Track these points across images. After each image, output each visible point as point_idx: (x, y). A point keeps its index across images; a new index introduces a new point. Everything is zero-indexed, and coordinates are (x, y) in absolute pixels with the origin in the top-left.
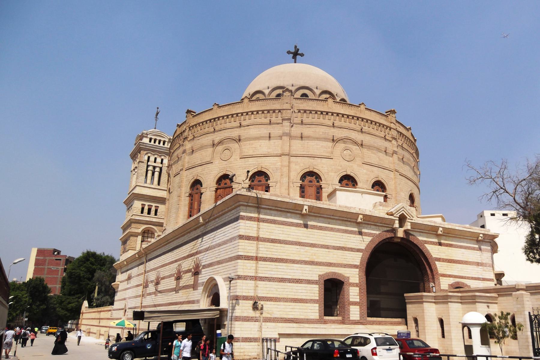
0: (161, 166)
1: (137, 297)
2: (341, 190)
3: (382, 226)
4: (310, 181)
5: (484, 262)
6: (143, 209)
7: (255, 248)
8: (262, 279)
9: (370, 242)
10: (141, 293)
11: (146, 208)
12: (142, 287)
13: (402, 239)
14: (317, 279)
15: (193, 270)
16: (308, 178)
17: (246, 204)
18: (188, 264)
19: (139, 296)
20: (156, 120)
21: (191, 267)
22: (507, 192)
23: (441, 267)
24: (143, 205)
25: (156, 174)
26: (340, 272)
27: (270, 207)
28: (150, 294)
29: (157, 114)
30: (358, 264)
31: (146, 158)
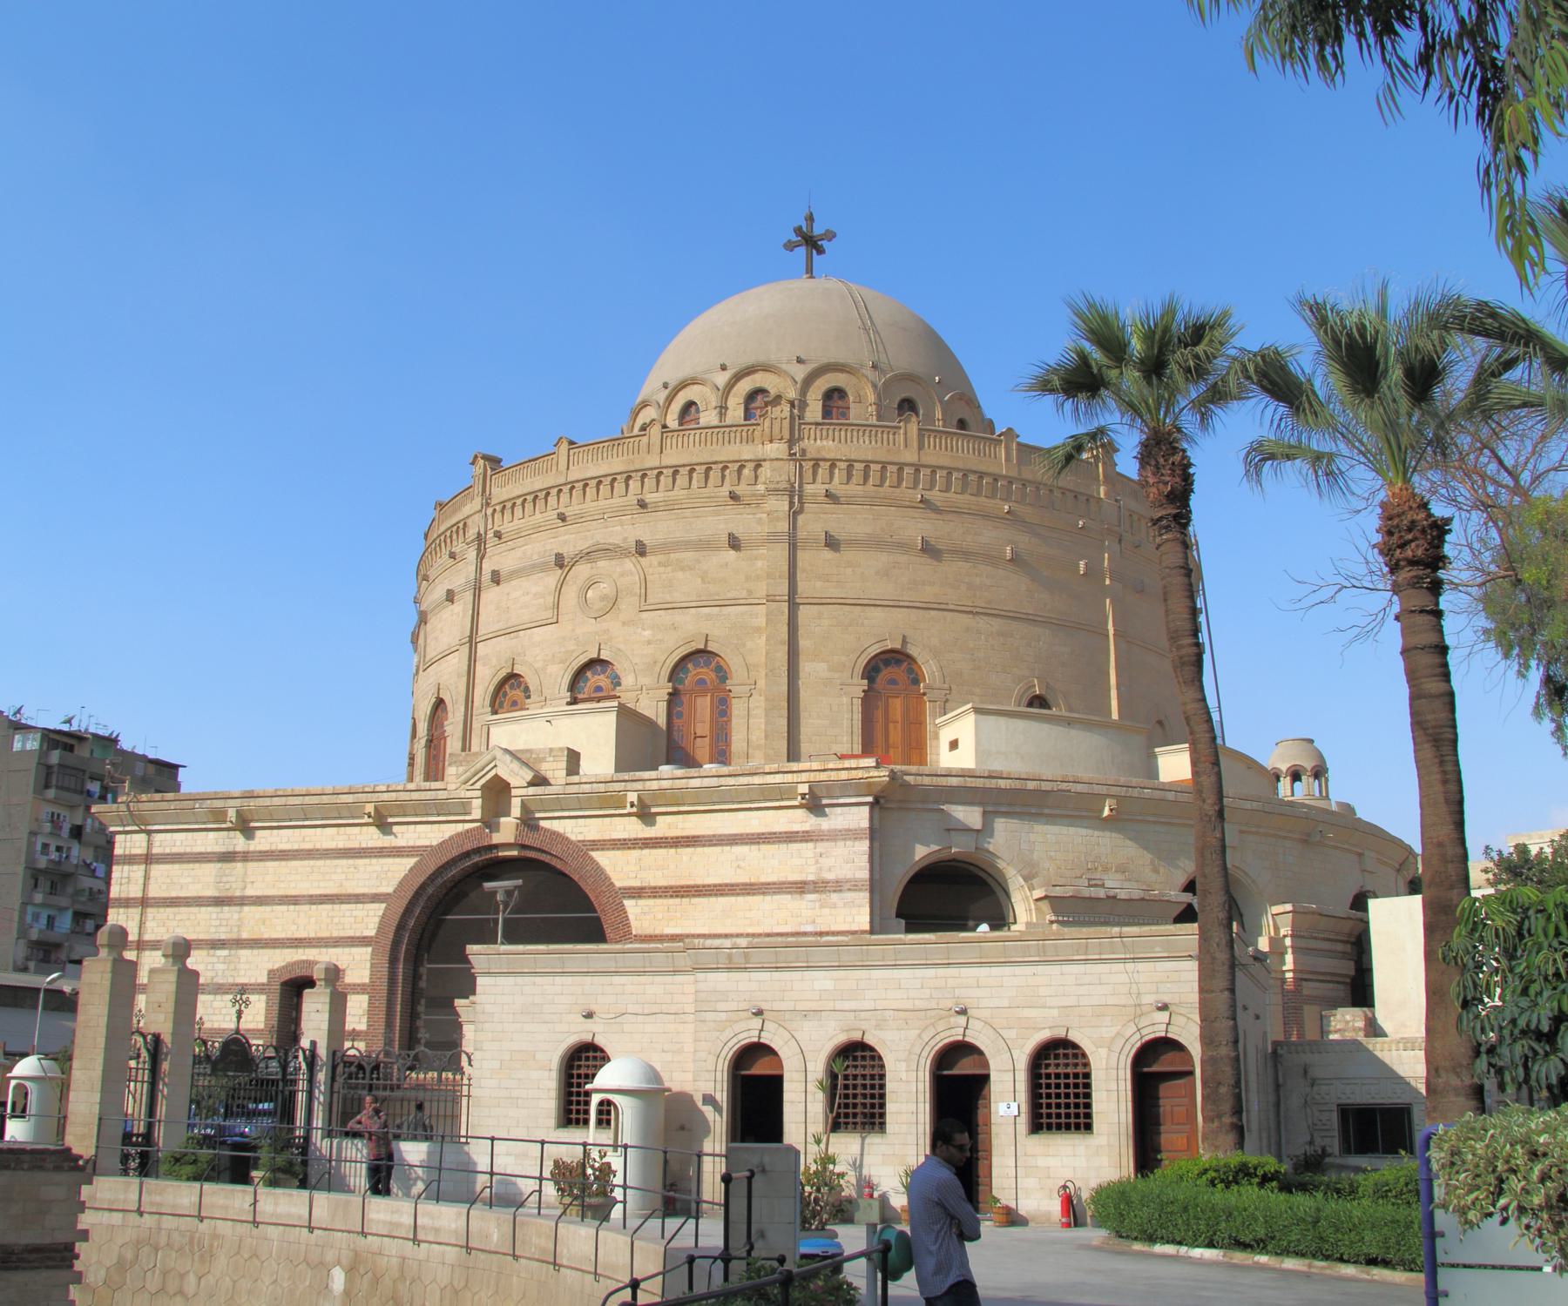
2: (497, 722)
5: (830, 876)
9: (411, 869)
14: (264, 980)
30: (372, 933)
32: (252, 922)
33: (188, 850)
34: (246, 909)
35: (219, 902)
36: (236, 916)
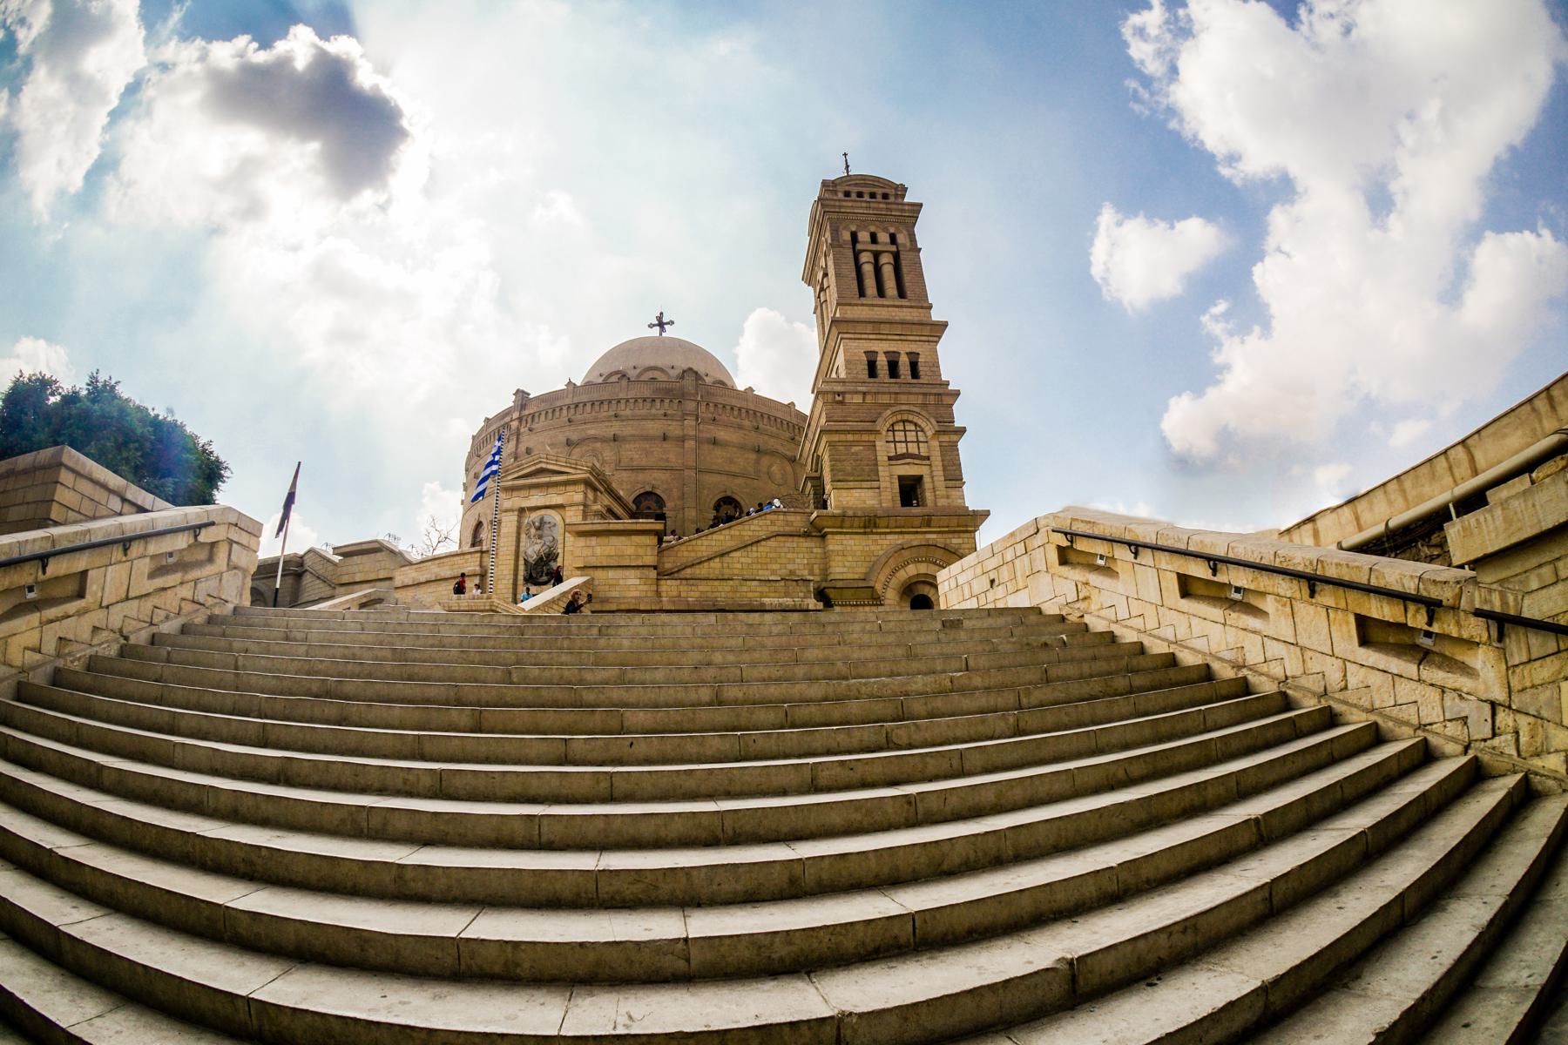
0: (894, 248)
11: (882, 361)
25: (888, 271)
31: (847, 236)
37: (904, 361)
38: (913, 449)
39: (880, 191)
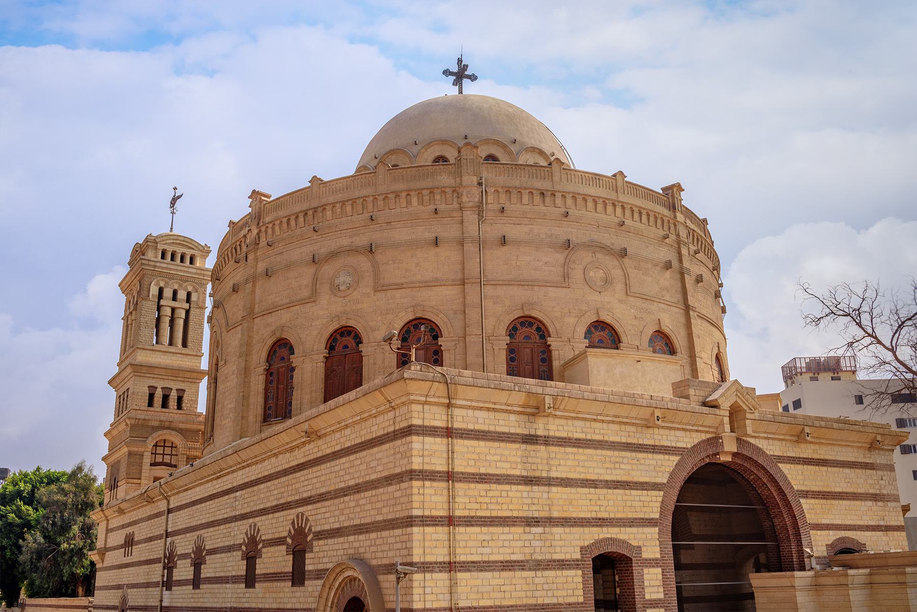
0: (187, 306)
1: (147, 585)
3: (697, 431)
4: (527, 337)
6: (151, 396)
7: (445, 499)
8: (468, 566)
10: (160, 579)
11: (159, 394)
12: (161, 565)
13: (735, 455)
14: (578, 556)
15: (289, 541)
16: (524, 330)
17: (423, 399)
18: (277, 526)
19: (156, 584)
20: (173, 213)
21: (285, 534)
22: (879, 342)
23: (811, 511)
24: (153, 389)
26: (622, 537)
27: (474, 404)
28: (180, 583)
29: (174, 200)
30: (656, 516)
31: (154, 291)
32: (562, 501)
33: (492, 428)
34: (554, 489)
35: (529, 481)
36: (545, 495)
37: (174, 395)
38: (167, 459)
39: (189, 252)
